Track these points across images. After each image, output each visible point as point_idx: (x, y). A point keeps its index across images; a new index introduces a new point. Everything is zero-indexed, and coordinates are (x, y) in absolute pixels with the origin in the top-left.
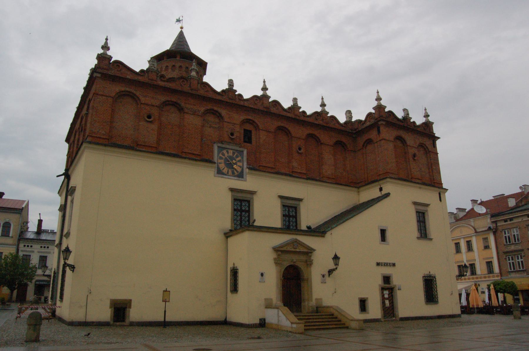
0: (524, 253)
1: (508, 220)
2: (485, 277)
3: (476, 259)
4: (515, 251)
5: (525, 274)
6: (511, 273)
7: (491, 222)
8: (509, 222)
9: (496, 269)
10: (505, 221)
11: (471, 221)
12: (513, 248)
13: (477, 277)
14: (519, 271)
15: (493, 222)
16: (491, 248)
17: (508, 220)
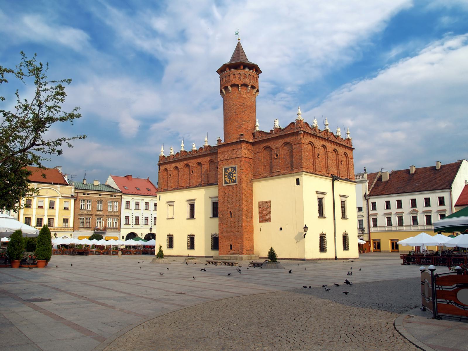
0: (92, 217)
1: (86, 194)
2: (61, 229)
3: (45, 215)
4: (87, 215)
5: (90, 230)
6: (81, 229)
7: (74, 192)
8: (86, 195)
9: (71, 224)
10: (84, 194)
11: (58, 187)
12: (86, 212)
13: (68, 229)
14: (87, 227)
15: (75, 192)
16: (55, 209)
17: (86, 194)
